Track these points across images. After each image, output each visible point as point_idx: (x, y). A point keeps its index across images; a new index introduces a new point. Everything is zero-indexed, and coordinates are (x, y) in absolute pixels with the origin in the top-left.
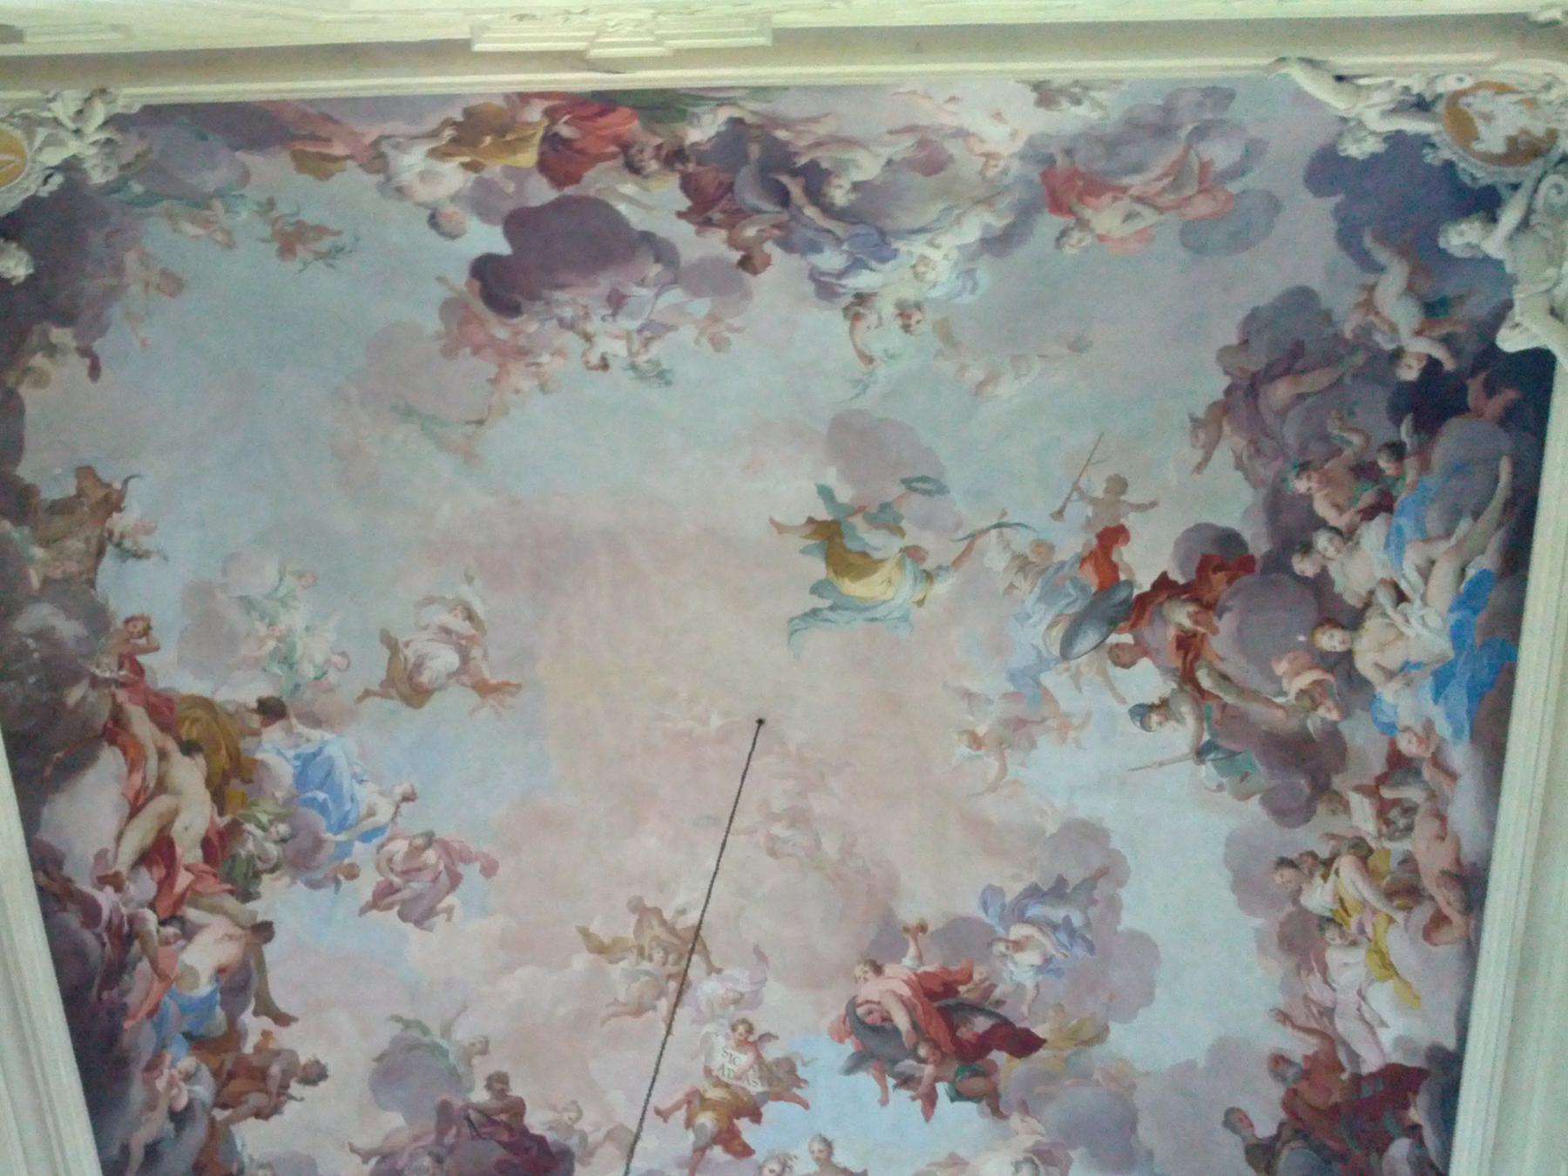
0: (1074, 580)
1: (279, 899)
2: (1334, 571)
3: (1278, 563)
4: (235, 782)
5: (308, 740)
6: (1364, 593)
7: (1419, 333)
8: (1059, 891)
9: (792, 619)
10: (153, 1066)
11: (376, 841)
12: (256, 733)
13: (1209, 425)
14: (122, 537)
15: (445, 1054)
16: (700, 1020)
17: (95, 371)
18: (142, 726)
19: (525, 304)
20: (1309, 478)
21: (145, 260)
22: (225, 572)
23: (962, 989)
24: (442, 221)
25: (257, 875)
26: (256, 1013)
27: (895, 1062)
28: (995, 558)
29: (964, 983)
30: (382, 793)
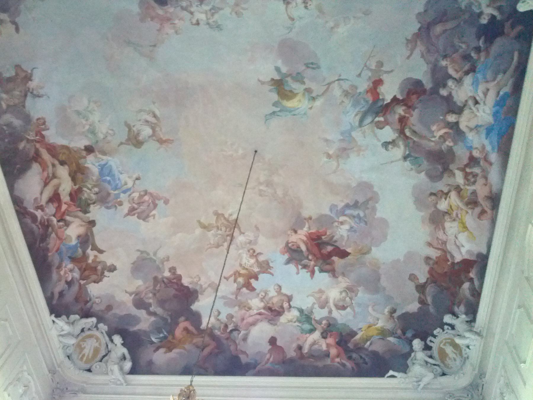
0: (364, 99)
2: (454, 93)
3: (435, 91)
5: (102, 160)
6: (464, 101)
7: (488, 6)
8: (356, 205)
9: (266, 115)
10: (59, 267)
11: (128, 193)
12: (85, 158)
13: (412, 42)
14: (33, 89)
15: (155, 261)
16: (238, 249)
18: (46, 155)
20: (447, 60)
23: (323, 237)
25: (89, 205)
26: (92, 250)
27: (301, 260)
28: (337, 92)
29: (324, 235)
30: (129, 177)
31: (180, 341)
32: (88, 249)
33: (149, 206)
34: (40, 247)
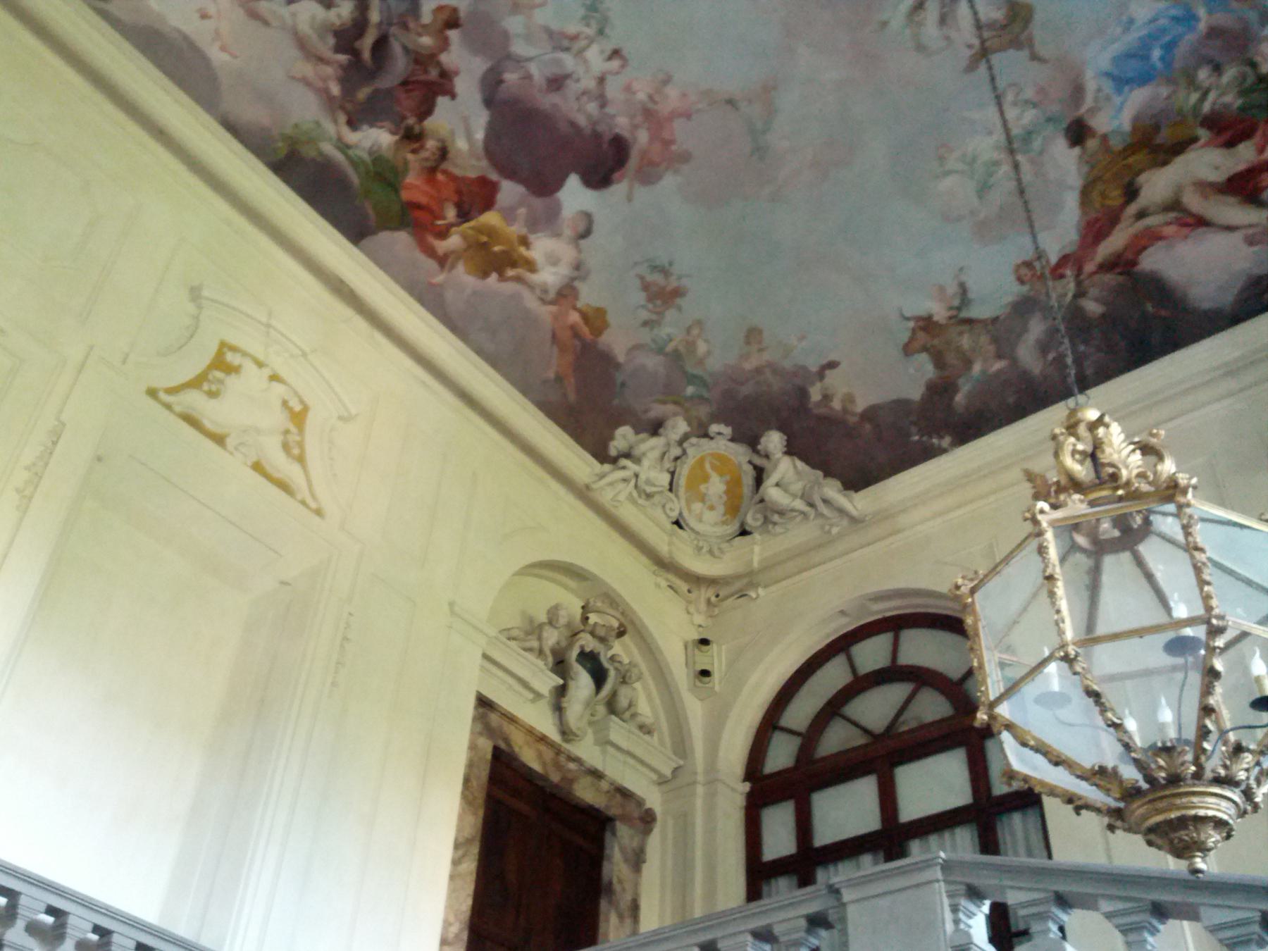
4: (1159, 140)
5: (1099, 90)
12: (1105, 138)
14: (951, 308)
17: (832, 365)
19: (607, 137)
24: (581, 228)
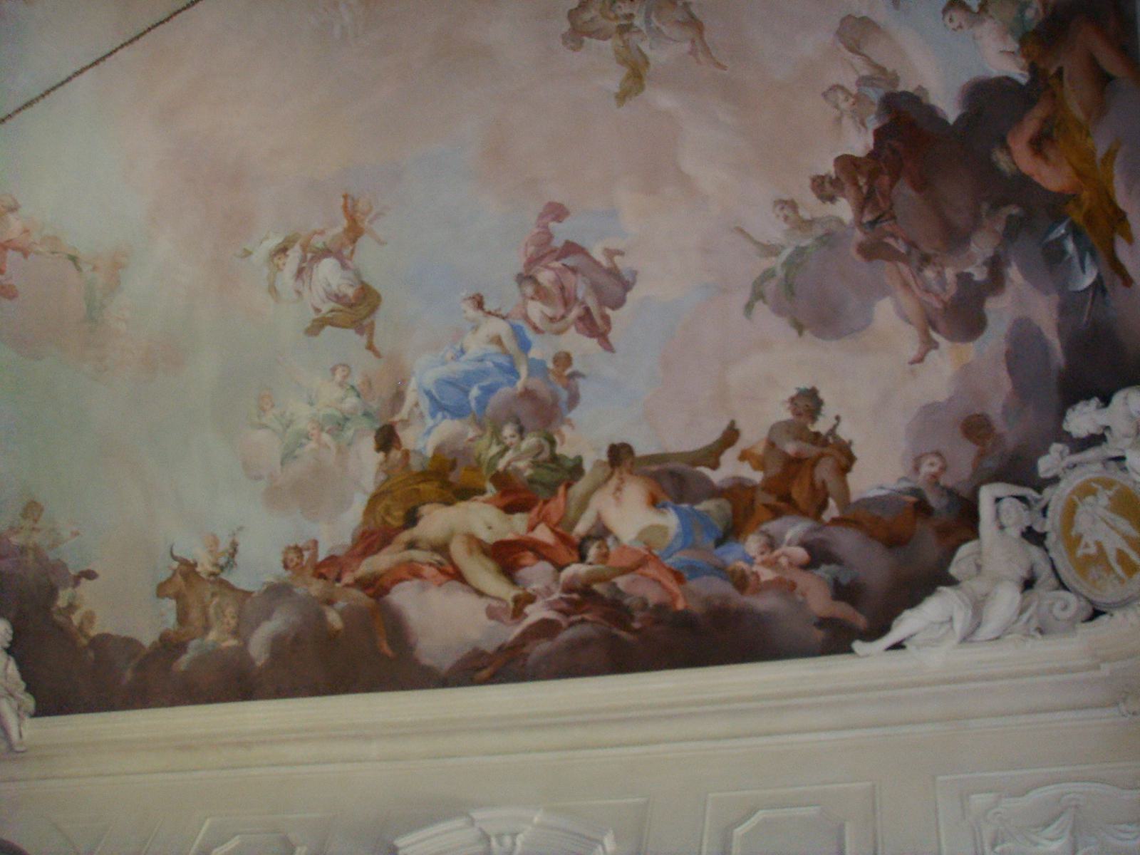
1: (584, 438)
4: (452, 477)
5: (417, 405)
10: (741, 582)
11: (530, 334)
12: (407, 454)
14: (216, 565)
15: (800, 252)
17: (90, 575)
21: (14, 530)
22: (258, 478)
25: (555, 458)
26: (715, 466)
30: (476, 328)
31: (1079, 174)
32: (706, 480)
33: (574, 270)
34: (635, 631)
